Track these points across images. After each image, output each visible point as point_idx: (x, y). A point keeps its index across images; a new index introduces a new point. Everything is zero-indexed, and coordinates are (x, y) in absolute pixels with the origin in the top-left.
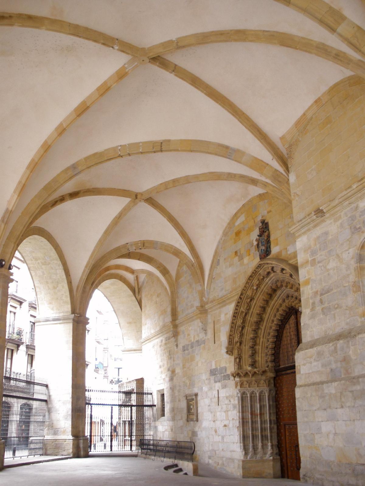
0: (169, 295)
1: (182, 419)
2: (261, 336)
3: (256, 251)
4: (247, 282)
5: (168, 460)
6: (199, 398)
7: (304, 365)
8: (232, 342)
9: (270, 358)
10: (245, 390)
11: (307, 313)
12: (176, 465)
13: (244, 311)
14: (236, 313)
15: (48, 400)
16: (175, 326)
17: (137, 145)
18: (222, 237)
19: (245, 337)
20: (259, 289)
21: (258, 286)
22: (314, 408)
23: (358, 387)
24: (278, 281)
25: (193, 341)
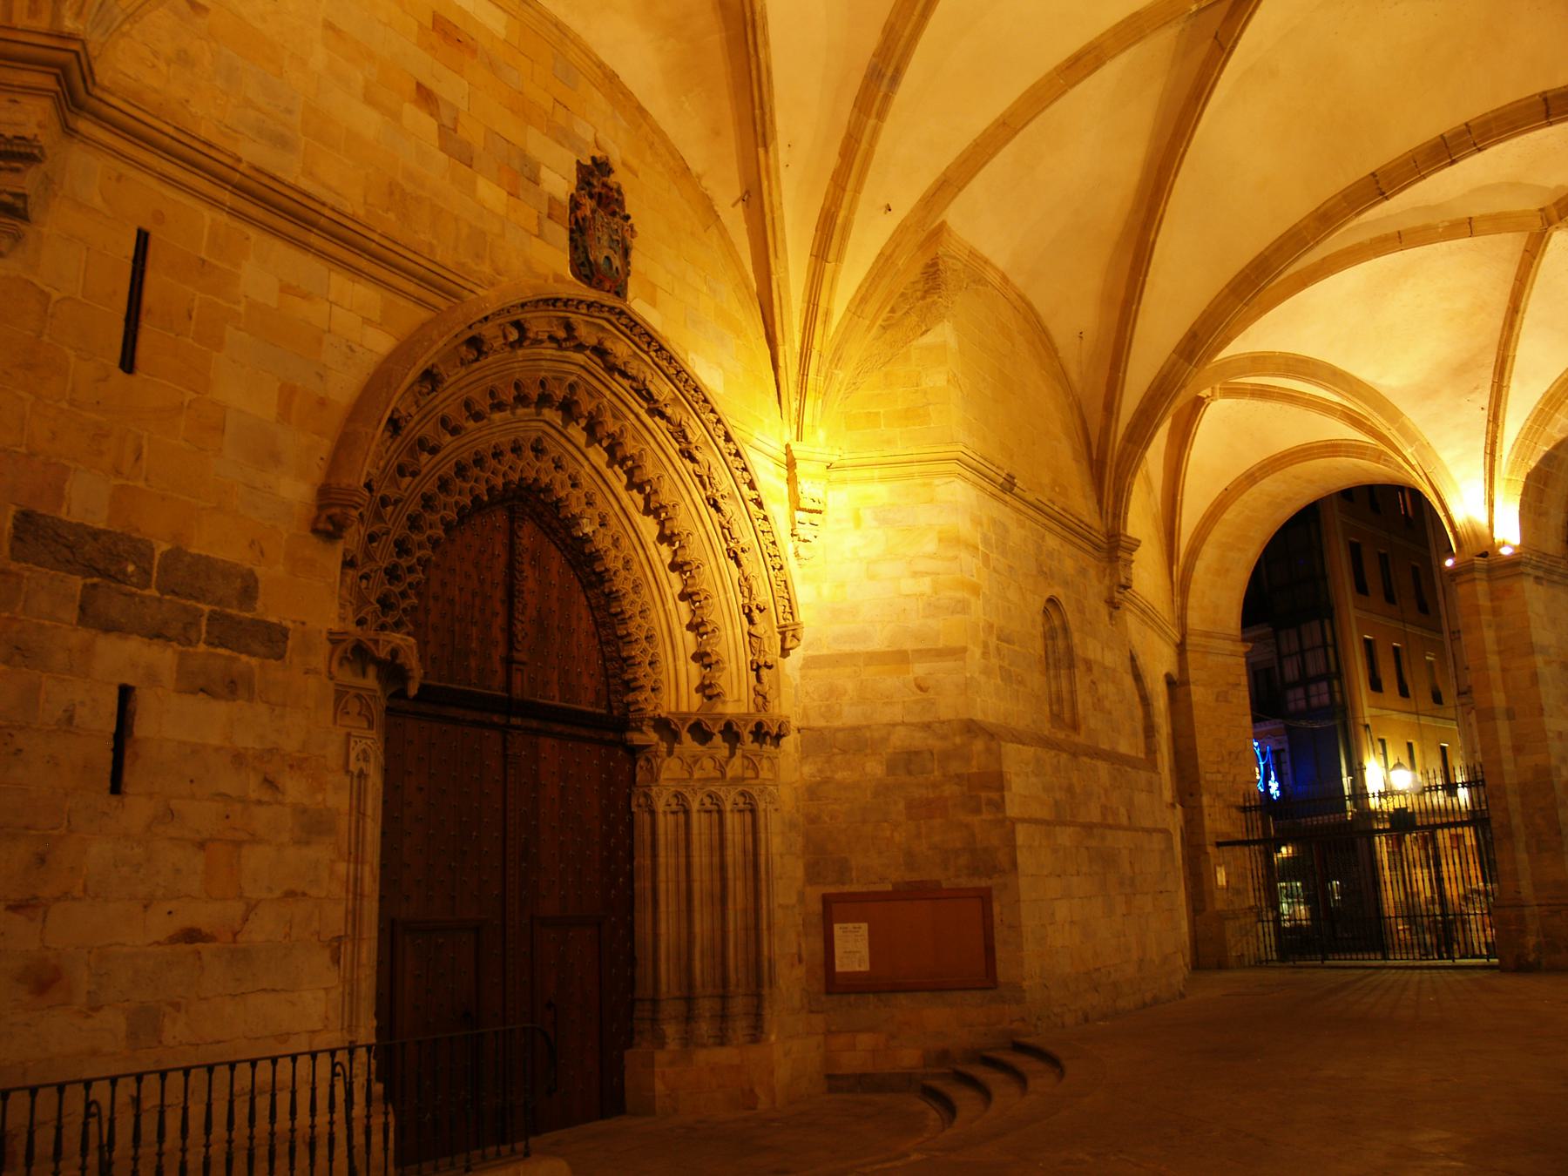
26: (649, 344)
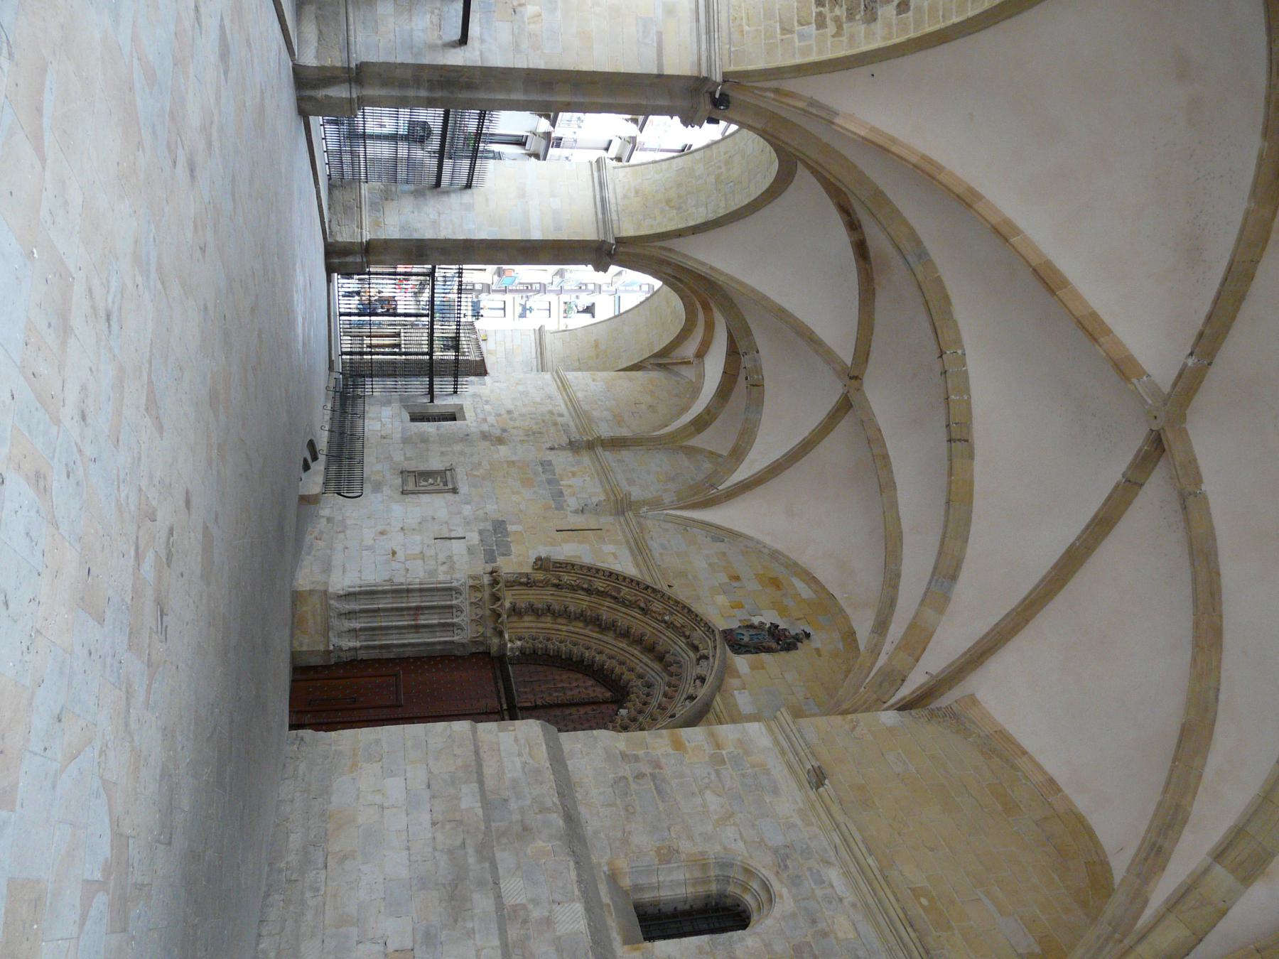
0: (654, 431)
1: (407, 459)
3: (740, 621)
4: (679, 603)
5: (326, 439)
6: (449, 496)
7: (516, 740)
8: (560, 569)
9: (528, 645)
11: (617, 745)
12: (315, 458)
13: (622, 594)
15: (439, 190)
16: (591, 446)
17: (965, 388)
18: (770, 549)
19: (570, 595)
20: (663, 625)
21: (670, 625)
22: (431, 763)
23: (472, 860)
24: (681, 667)
25: (562, 483)
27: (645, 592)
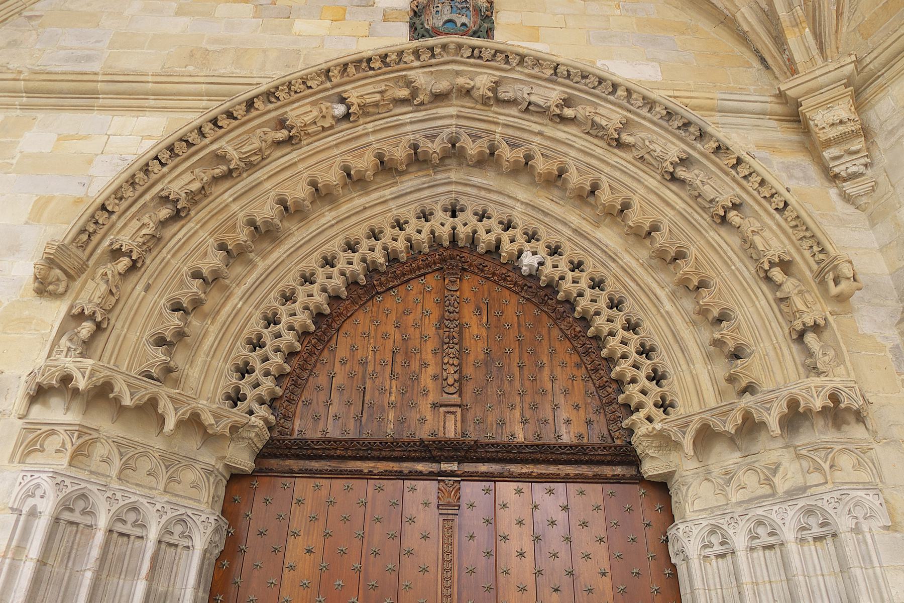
2: (239, 292)
10: (94, 488)
14: (187, 141)
19: (165, 251)
26: (507, 62)
27: (254, 113)
